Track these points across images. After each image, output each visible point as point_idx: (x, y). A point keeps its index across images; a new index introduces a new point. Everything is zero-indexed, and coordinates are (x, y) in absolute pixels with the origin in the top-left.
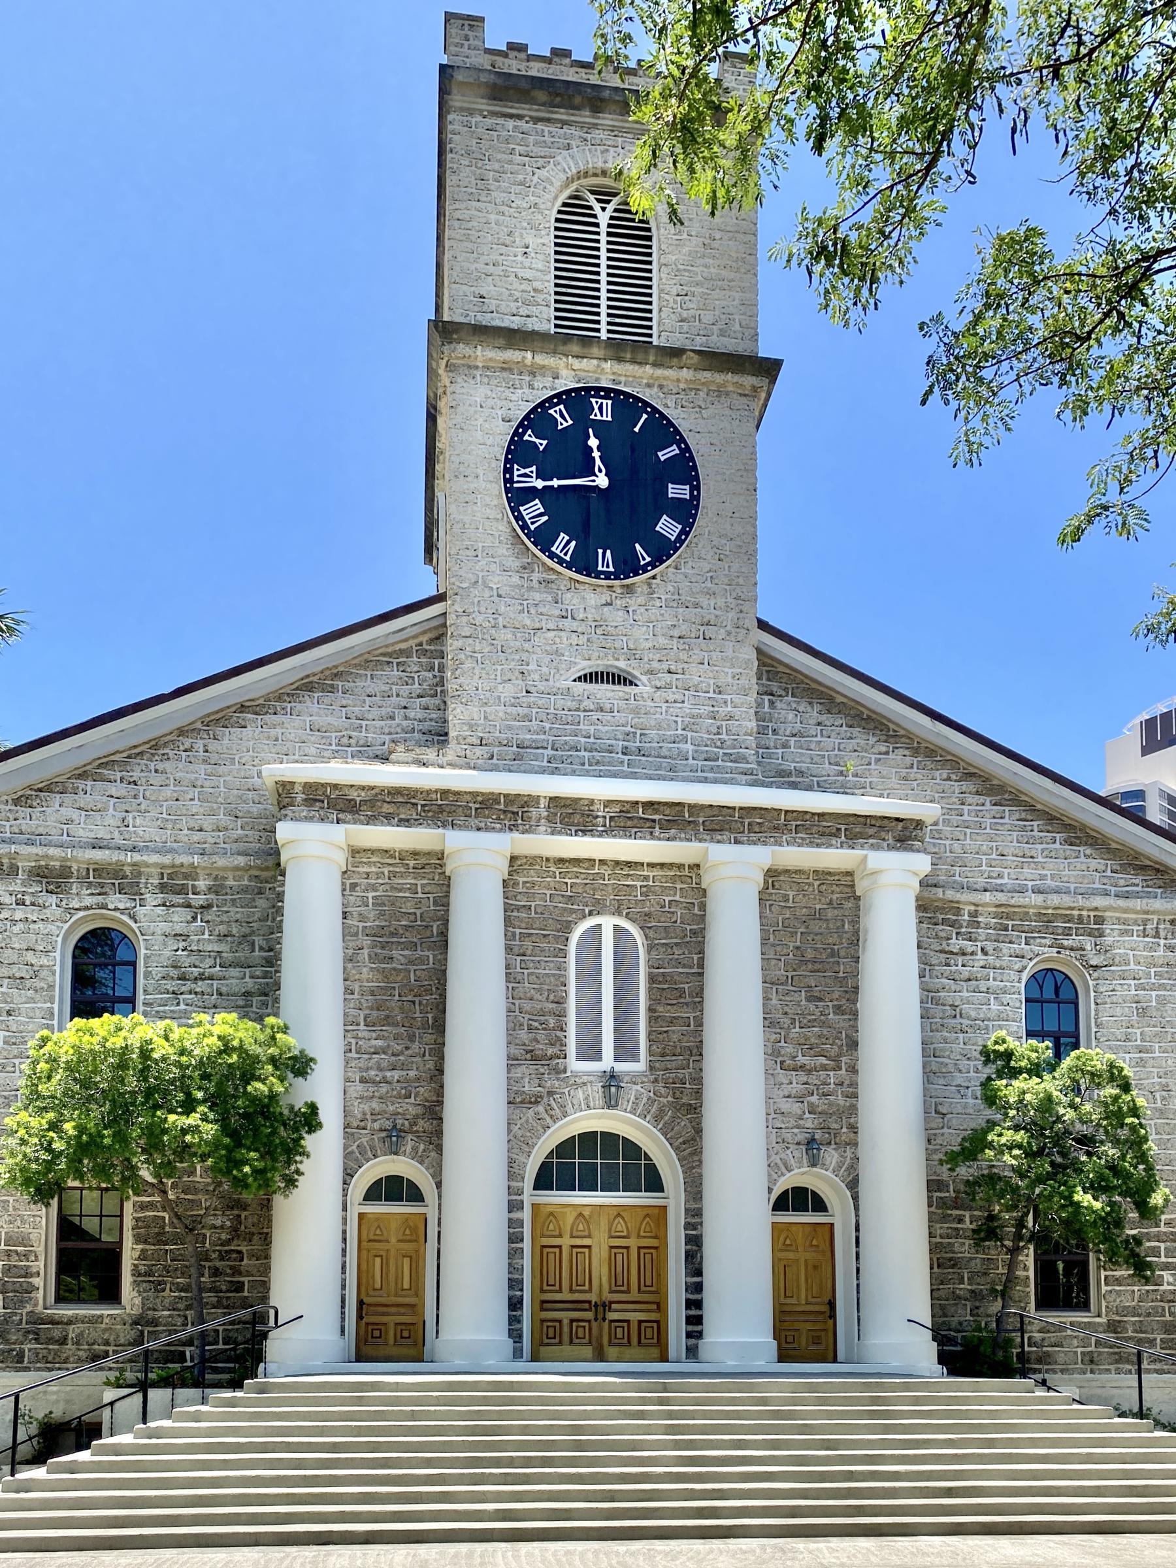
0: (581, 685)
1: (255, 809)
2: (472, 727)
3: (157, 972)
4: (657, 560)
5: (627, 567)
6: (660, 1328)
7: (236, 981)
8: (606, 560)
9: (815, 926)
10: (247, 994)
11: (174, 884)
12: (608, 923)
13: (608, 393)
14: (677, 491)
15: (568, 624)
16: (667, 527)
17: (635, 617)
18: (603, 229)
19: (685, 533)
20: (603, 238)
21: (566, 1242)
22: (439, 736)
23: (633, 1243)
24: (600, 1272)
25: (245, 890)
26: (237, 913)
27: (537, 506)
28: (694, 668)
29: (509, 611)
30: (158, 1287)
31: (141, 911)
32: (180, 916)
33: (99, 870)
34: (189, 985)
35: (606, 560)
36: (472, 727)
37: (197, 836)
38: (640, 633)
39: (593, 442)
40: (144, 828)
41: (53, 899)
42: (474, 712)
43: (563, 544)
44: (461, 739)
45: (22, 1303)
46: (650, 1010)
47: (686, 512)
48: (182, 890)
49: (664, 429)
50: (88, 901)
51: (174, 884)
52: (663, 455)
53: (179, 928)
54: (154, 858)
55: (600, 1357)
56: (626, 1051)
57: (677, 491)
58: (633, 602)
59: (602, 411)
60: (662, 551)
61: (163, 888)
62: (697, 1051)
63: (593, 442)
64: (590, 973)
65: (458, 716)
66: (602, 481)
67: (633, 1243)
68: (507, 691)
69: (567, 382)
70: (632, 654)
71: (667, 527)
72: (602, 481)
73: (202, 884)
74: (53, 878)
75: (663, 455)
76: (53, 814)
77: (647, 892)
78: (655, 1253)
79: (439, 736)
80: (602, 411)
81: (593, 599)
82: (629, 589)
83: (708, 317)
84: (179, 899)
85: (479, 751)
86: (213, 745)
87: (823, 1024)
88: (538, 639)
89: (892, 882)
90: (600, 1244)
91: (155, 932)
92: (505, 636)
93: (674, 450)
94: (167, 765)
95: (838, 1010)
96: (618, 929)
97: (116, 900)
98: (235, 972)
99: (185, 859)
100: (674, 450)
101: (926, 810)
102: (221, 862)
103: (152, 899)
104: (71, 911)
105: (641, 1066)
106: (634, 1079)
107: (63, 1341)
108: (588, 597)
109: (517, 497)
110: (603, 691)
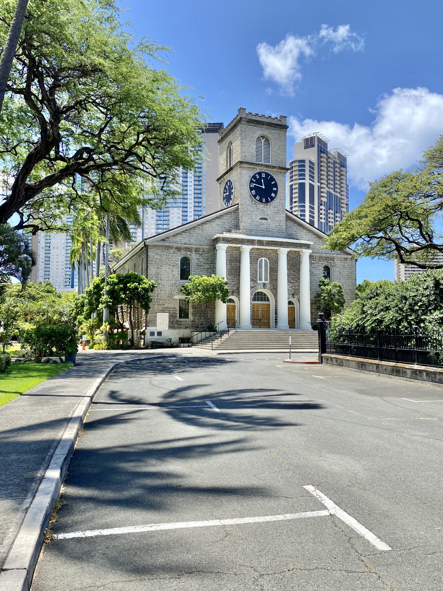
0: (260, 220)
1: (209, 238)
2: (244, 227)
3: (195, 265)
4: (272, 200)
5: (267, 201)
6: (269, 323)
7: (207, 266)
8: (264, 200)
9: (294, 260)
10: (208, 268)
11: (197, 250)
12: (263, 259)
13: (264, 173)
14: (274, 189)
15: (258, 210)
16: (273, 195)
17: (269, 209)
18: (263, 143)
19: (276, 196)
20: (263, 145)
21: (255, 309)
22: (237, 227)
23: (265, 310)
24: (260, 314)
25: (207, 251)
26: (206, 255)
27: (254, 191)
28: (277, 218)
29: (249, 208)
30: (195, 316)
31: (192, 255)
32: (198, 255)
33: (186, 248)
34: (199, 267)
35: (264, 200)
36: (244, 227)
37: (200, 242)
38: (269, 212)
39: (262, 181)
40: (192, 241)
41: (179, 252)
42: (244, 224)
43: (258, 198)
44: (242, 229)
45: (175, 318)
46: (270, 273)
47: (276, 192)
48: (198, 251)
49: (272, 179)
50: (184, 253)
51: (197, 250)
52: (272, 183)
53: (198, 258)
54: (195, 246)
55: (260, 327)
56: (266, 280)
57: (274, 189)
58: (268, 207)
59: (264, 175)
60: (272, 199)
61: (195, 251)
62: (277, 280)
63: (262, 181)
64: (261, 267)
65: (242, 225)
66: (264, 187)
67: (265, 310)
68: (249, 221)
69: (258, 171)
70: (268, 215)
71: (273, 195)
72: (264, 187)
73: (201, 250)
74: (179, 249)
75: (272, 183)
76: (179, 238)
77: (269, 254)
78: (269, 311)
79: (237, 227)
80: (264, 175)
81: (262, 206)
82: (267, 205)
83: (279, 160)
84: (198, 253)
85: (245, 231)
86: (202, 227)
87: (295, 275)
88: (254, 213)
89: (306, 253)
90: (260, 310)
91: (194, 258)
92: (249, 212)
93: (274, 182)
94: (196, 231)
95: (297, 273)
96: (265, 260)
97: (188, 253)
98: (206, 265)
99: (199, 247)
100: (274, 182)
101: (311, 243)
102: (205, 247)
103: (194, 253)
104: (181, 254)
105: (268, 282)
106: (267, 283)
107: (181, 325)
108: (261, 206)
109: (251, 189)
110: (263, 221)
